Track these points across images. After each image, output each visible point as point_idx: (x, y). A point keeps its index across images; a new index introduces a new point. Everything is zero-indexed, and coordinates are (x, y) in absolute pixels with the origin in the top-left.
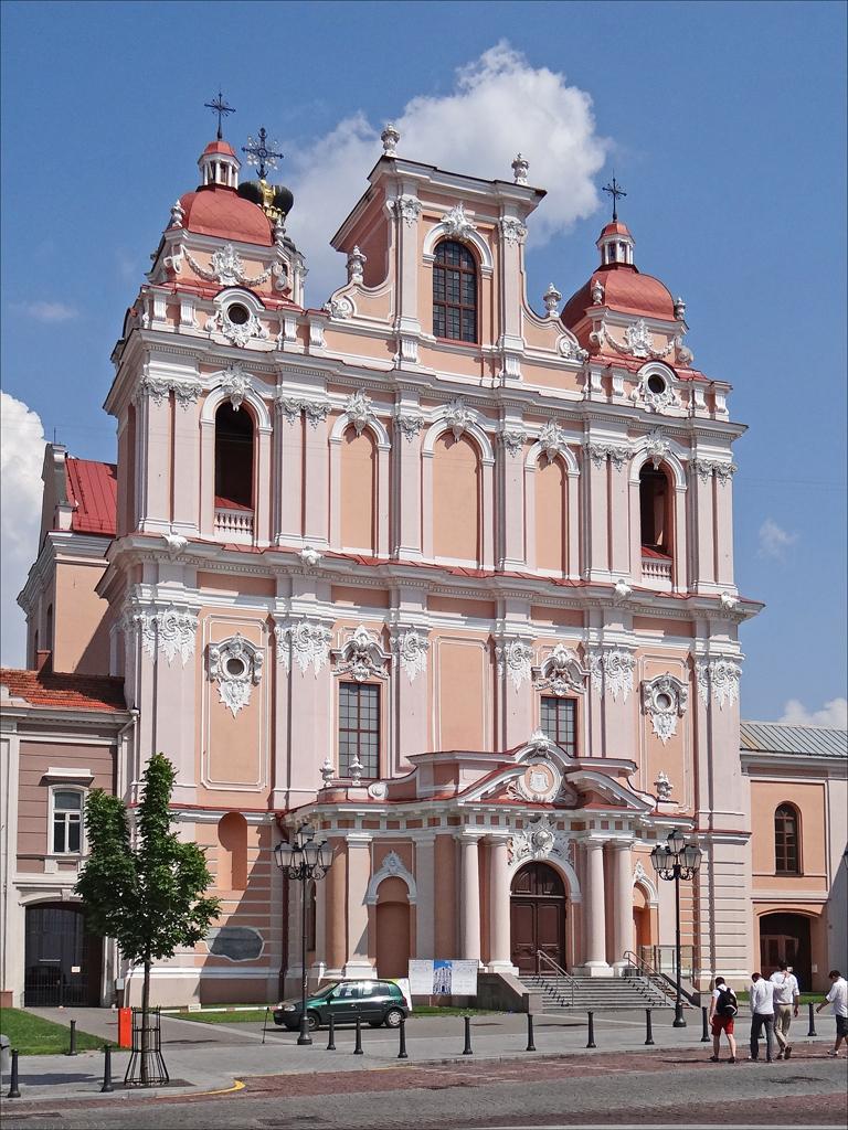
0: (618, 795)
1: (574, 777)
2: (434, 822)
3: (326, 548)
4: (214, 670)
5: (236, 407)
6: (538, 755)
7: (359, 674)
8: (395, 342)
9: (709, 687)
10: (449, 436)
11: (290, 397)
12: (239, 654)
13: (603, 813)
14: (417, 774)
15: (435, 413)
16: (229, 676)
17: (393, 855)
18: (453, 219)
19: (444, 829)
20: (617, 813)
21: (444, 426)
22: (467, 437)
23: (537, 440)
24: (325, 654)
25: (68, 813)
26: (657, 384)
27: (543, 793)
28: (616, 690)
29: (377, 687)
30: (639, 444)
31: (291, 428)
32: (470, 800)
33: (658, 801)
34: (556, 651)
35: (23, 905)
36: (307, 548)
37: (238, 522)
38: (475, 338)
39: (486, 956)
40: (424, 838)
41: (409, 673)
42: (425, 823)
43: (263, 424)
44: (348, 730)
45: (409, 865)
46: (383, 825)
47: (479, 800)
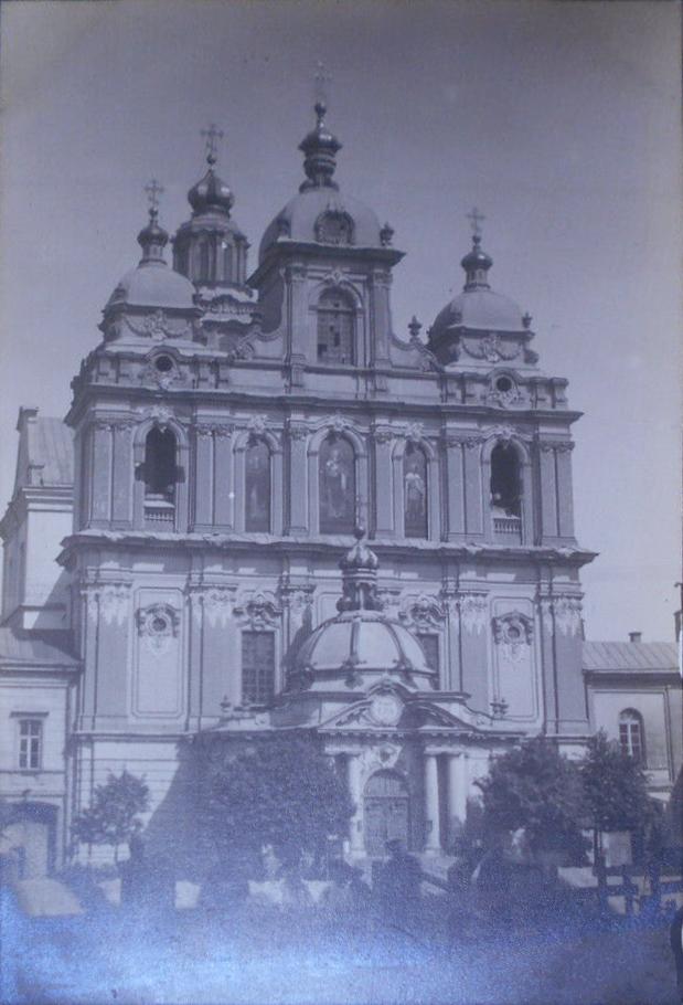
4: (142, 628)
7: (257, 625)
8: (286, 370)
9: (554, 620)
10: (332, 437)
12: (163, 615)
15: (315, 420)
18: (333, 277)
22: (344, 436)
24: (229, 613)
28: (470, 628)
29: (272, 634)
30: (488, 430)
31: (205, 441)
34: (419, 598)
38: (353, 361)
43: (182, 440)
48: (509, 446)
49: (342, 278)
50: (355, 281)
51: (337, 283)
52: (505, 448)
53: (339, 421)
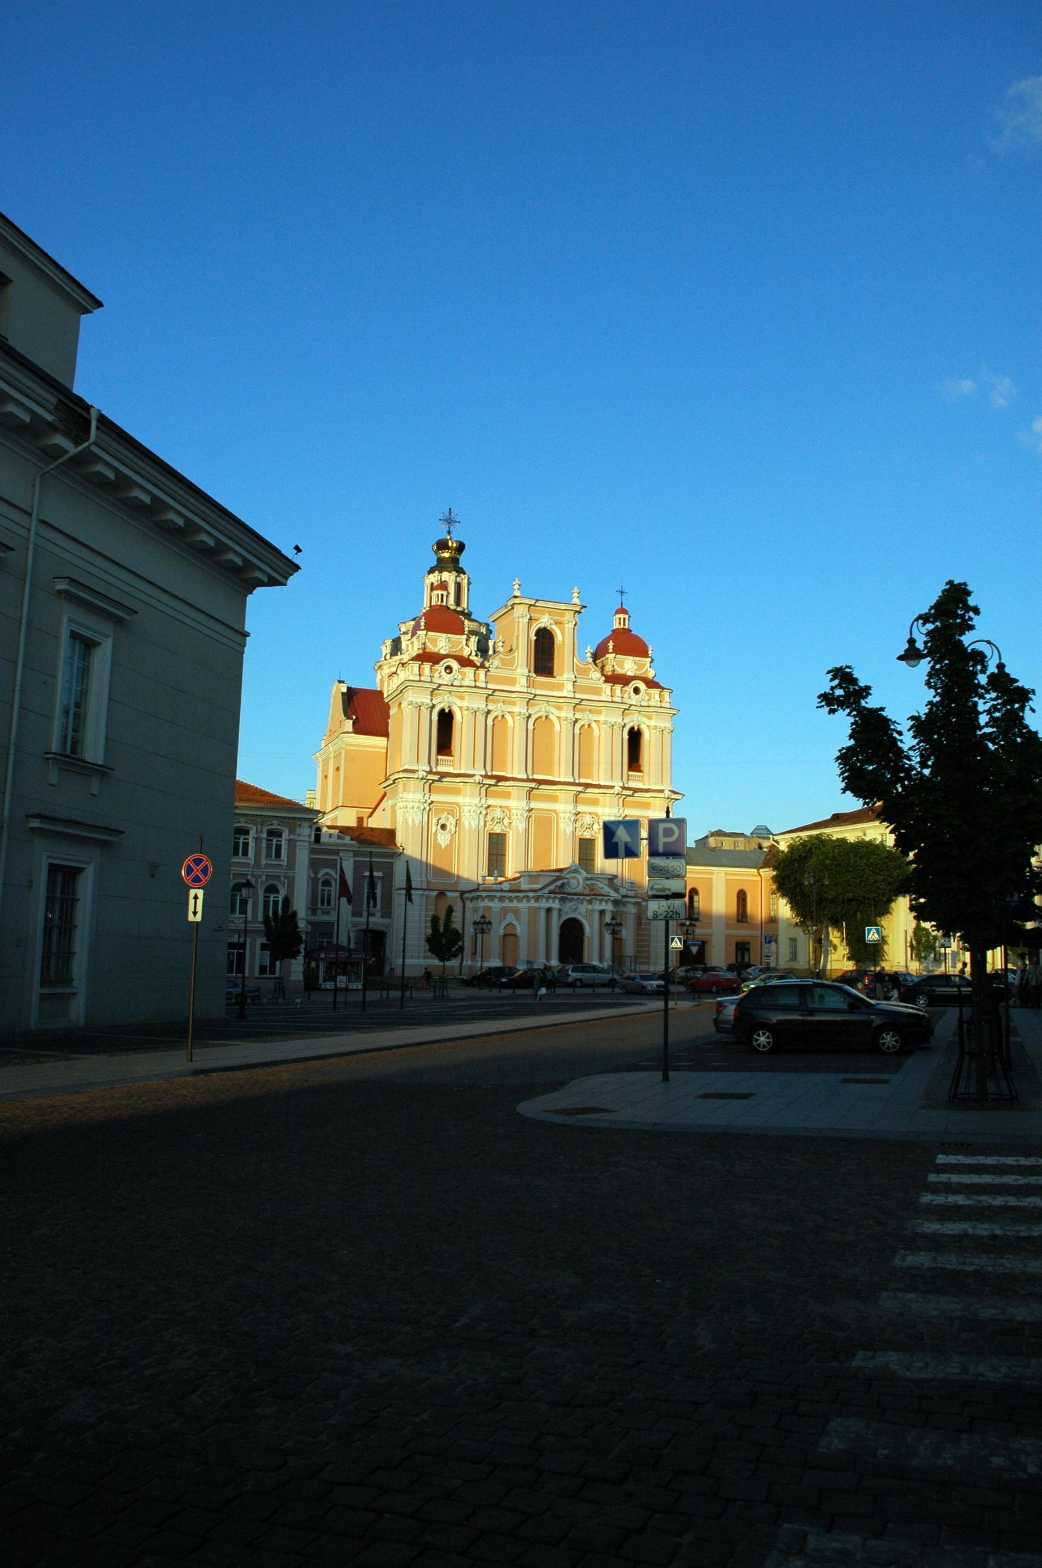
1: (589, 882)
2: (528, 900)
3: (483, 773)
5: (447, 710)
13: (600, 898)
14: (522, 879)
16: (442, 831)
17: (511, 914)
19: (533, 904)
20: (606, 898)
33: (628, 890)
39: (548, 957)
40: (524, 905)
42: (525, 901)
45: (517, 918)
46: (507, 901)
48: (638, 729)
52: (636, 729)
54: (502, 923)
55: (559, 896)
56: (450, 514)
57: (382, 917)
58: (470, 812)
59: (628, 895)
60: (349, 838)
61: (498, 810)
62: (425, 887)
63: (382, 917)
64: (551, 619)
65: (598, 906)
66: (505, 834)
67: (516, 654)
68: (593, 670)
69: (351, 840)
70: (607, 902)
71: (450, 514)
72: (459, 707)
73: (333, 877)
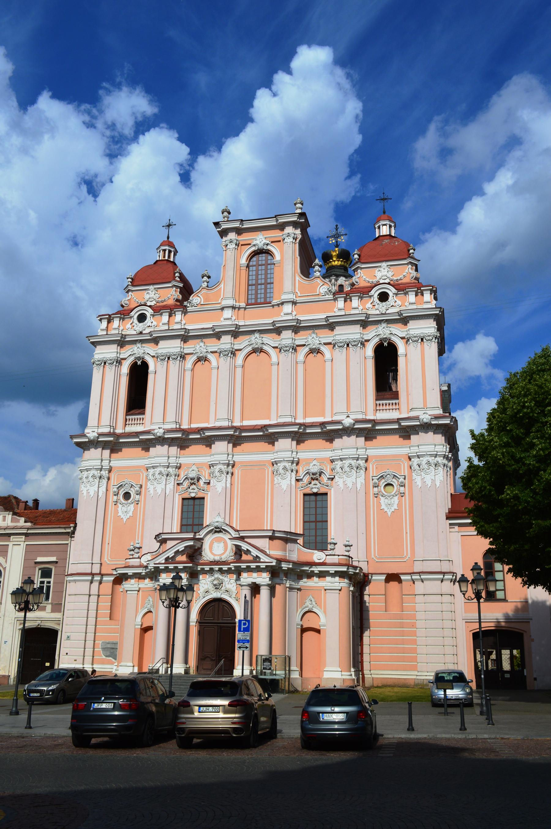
0: (255, 552)
5: (139, 363)
6: (216, 532)
11: (160, 352)
13: (243, 566)
20: (253, 565)
21: (250, 349)
22: (261, 351)
23: (304, 345)
25: (46, 580)
26: (384, 297)
27: (218, 555)
28: (350, 485)
32: (157, 562)
34: (312, 465)
35: (19, 629)
36: (159, 428)
37: (141, 420)
41: (218, 489)
44: (187, 525)
47: (163, 562)
48: (388, 344)
49: (264, 241)
50: (272, 242)
51: (261, 245)
53: (256, 340)
54: (139, 611)
55: (180, 566)
56: (337, 230)
57: (53, 611)
58: (153, 475)
59: (328, 561)
60: (23, 519)
61: (194, 467)
62: (96, 570)
63: (53, 611)
64: (266, 238)
65: (247, 578)
66: (203, 498)
67: (222, 285)
68: (322, 284)
69: (25, 522)
70: (258, 569)
71: (337, 230)
72: (153, 357)
73: (2, 567)
